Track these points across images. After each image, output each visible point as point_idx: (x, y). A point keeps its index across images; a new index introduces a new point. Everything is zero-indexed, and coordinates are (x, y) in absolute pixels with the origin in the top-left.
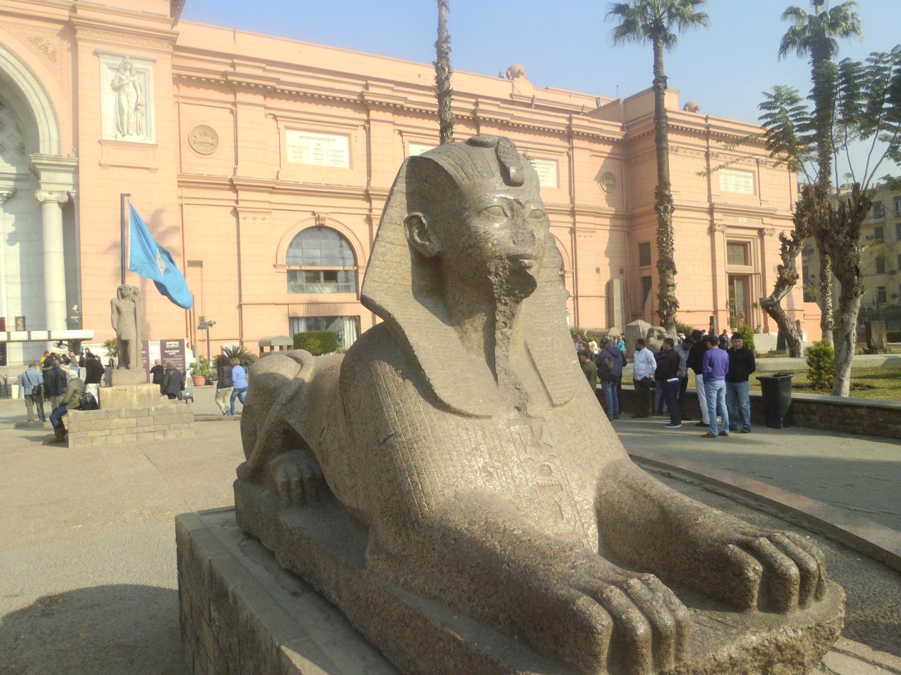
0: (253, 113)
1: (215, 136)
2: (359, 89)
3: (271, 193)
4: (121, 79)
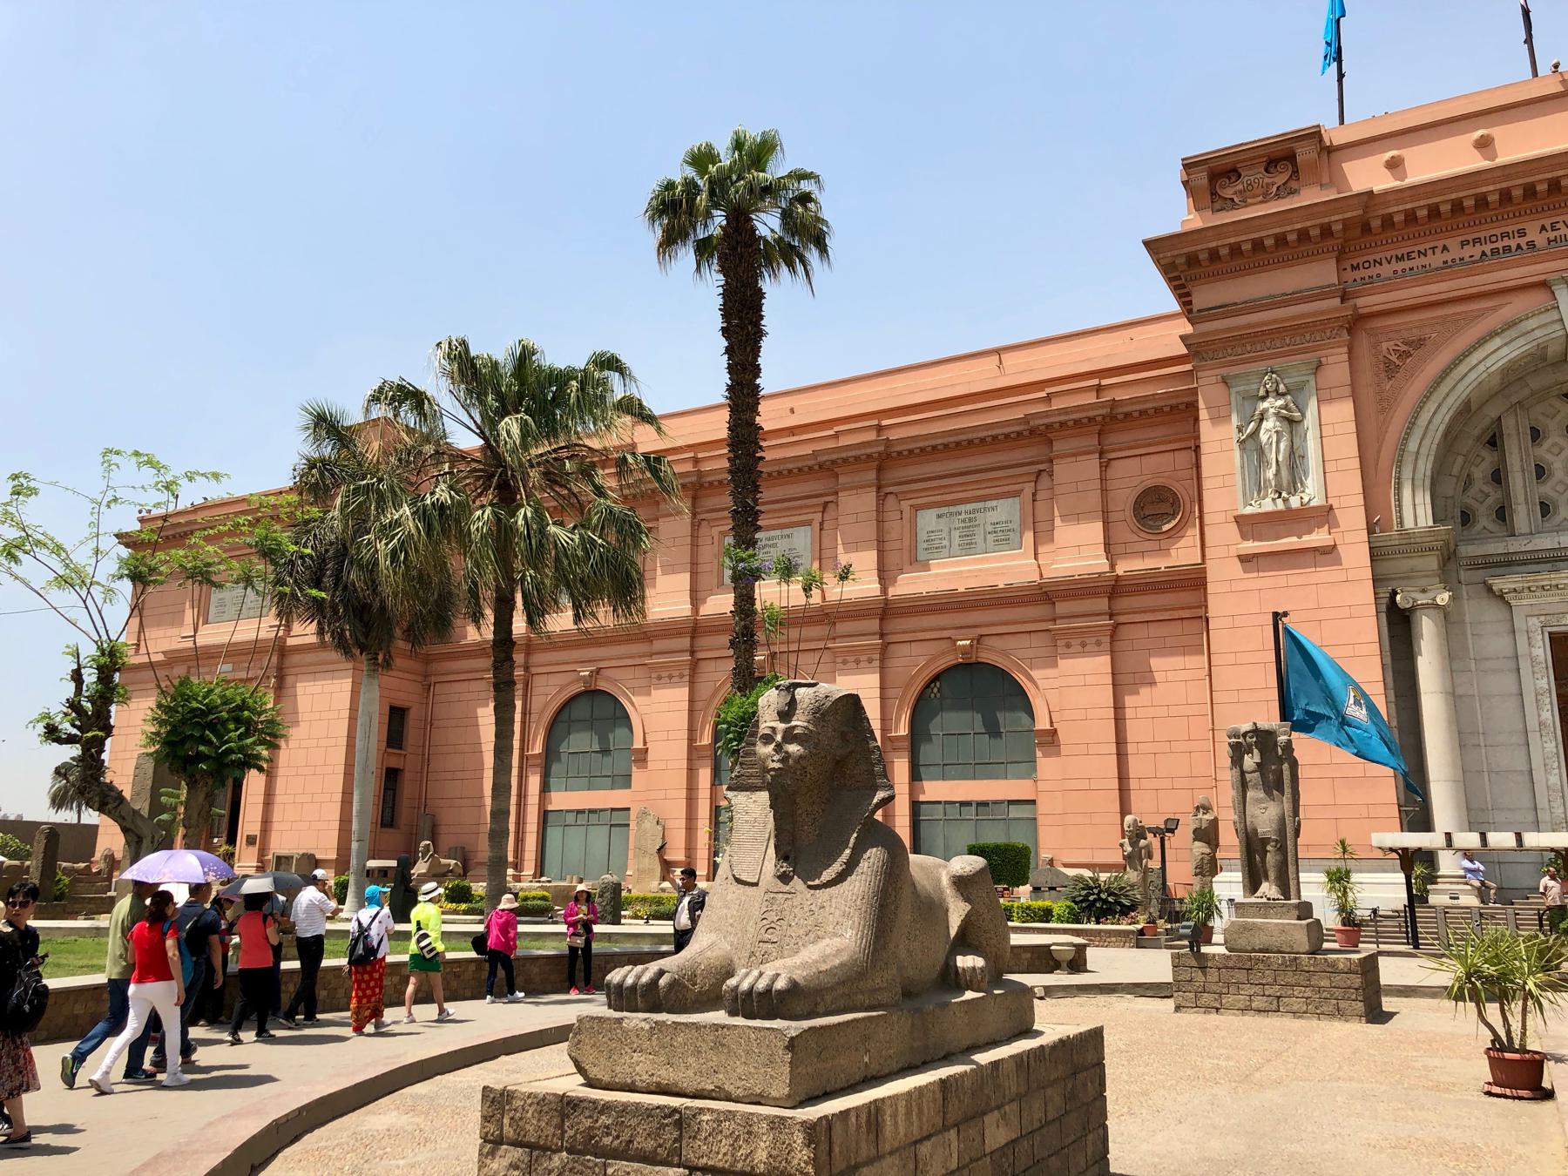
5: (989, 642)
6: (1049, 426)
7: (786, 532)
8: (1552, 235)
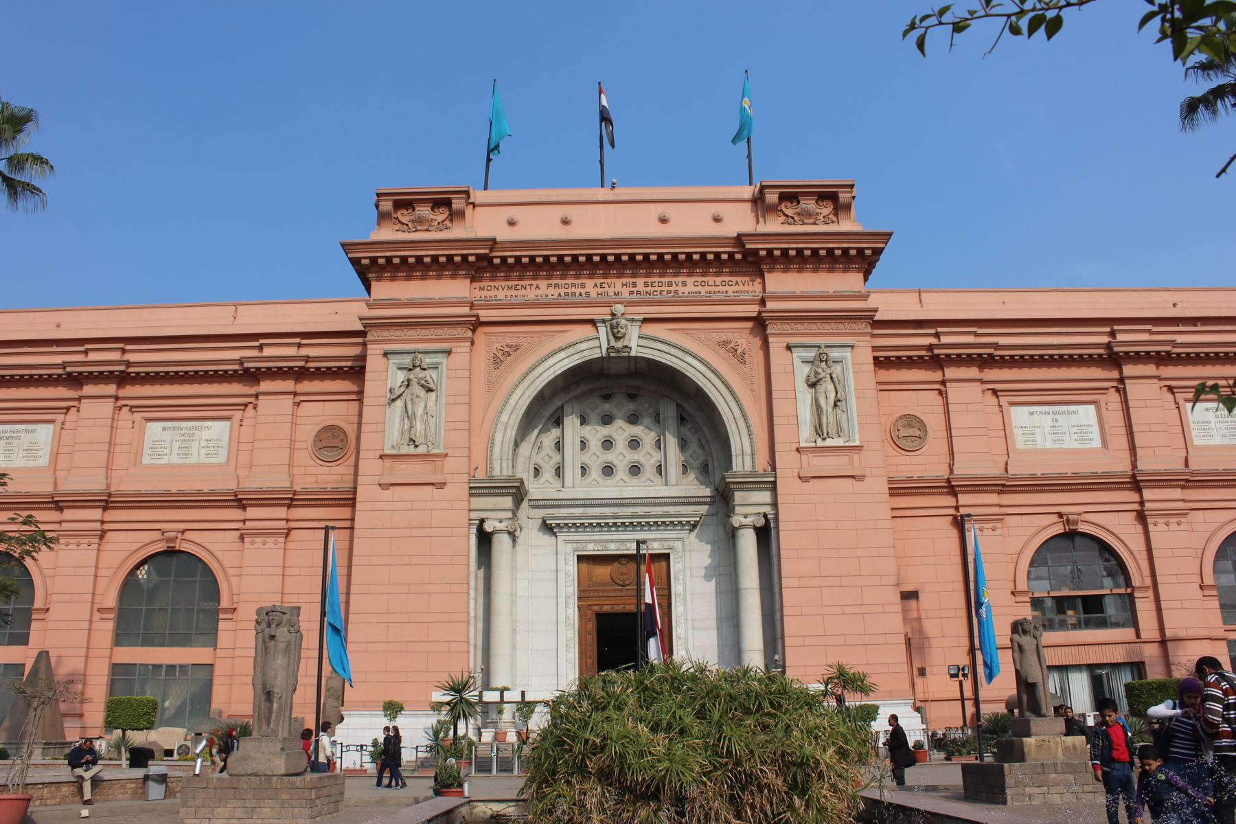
0: (967, 392)
1: (923, 426)
2: (1105, 339)
3: (1000, 492)
4: (817, 373)
5: (188, 535)
6: (258, 369)
7: (31, 427)
8: (600, 290)
